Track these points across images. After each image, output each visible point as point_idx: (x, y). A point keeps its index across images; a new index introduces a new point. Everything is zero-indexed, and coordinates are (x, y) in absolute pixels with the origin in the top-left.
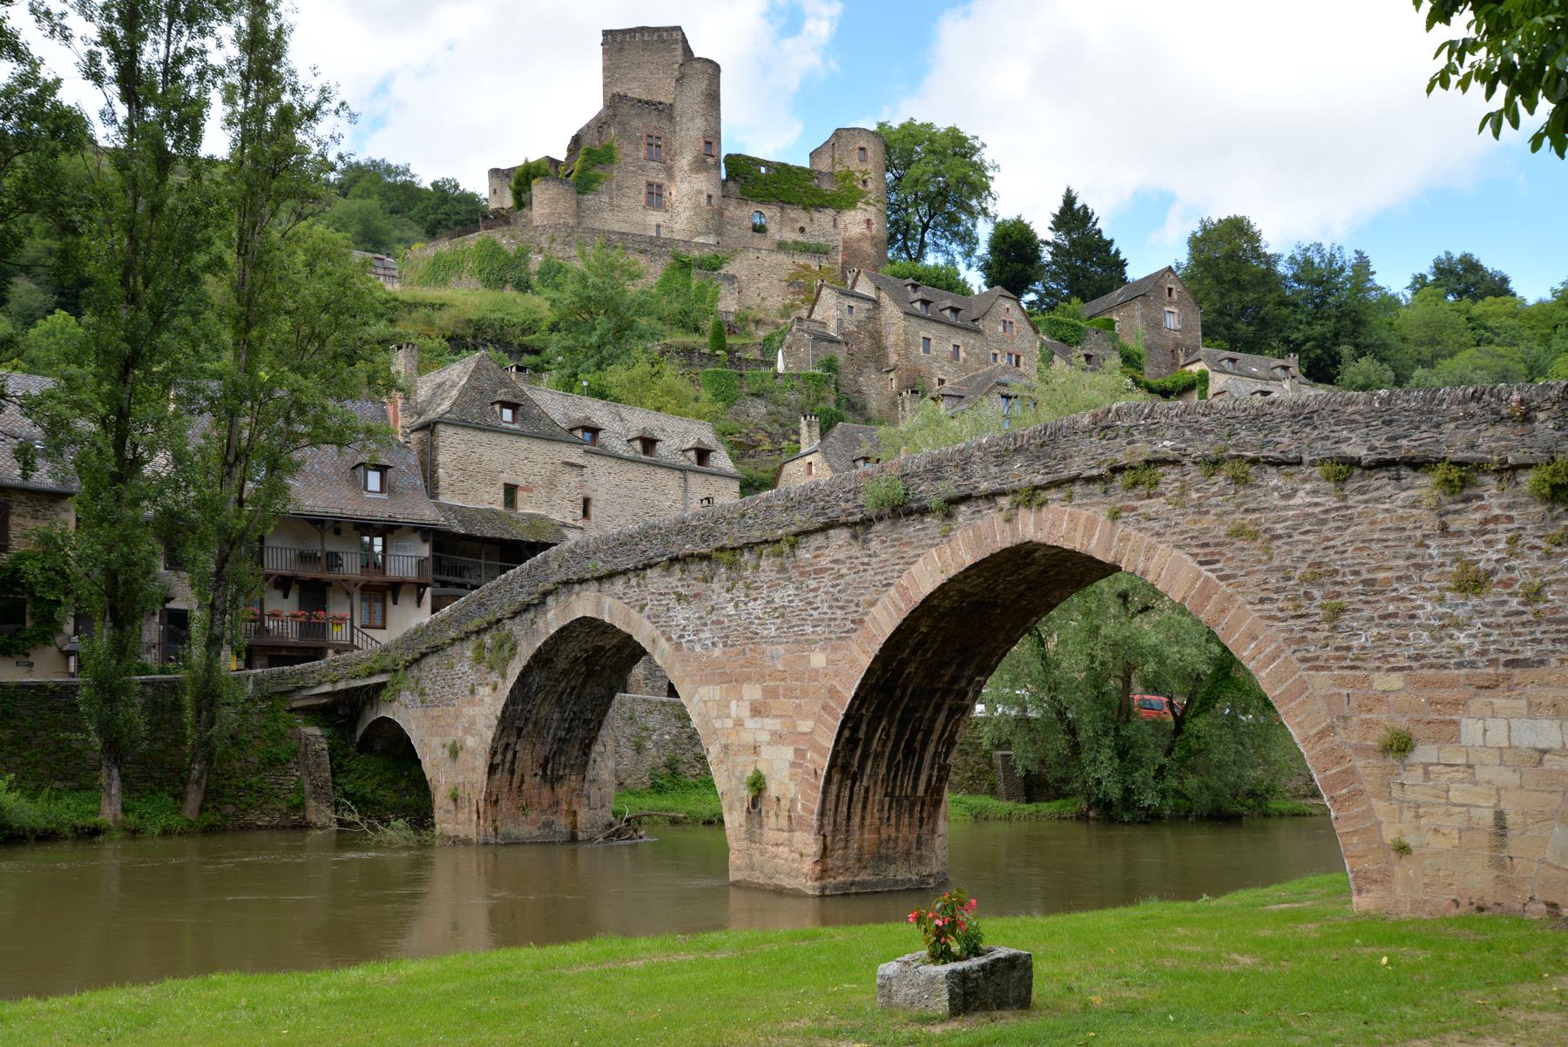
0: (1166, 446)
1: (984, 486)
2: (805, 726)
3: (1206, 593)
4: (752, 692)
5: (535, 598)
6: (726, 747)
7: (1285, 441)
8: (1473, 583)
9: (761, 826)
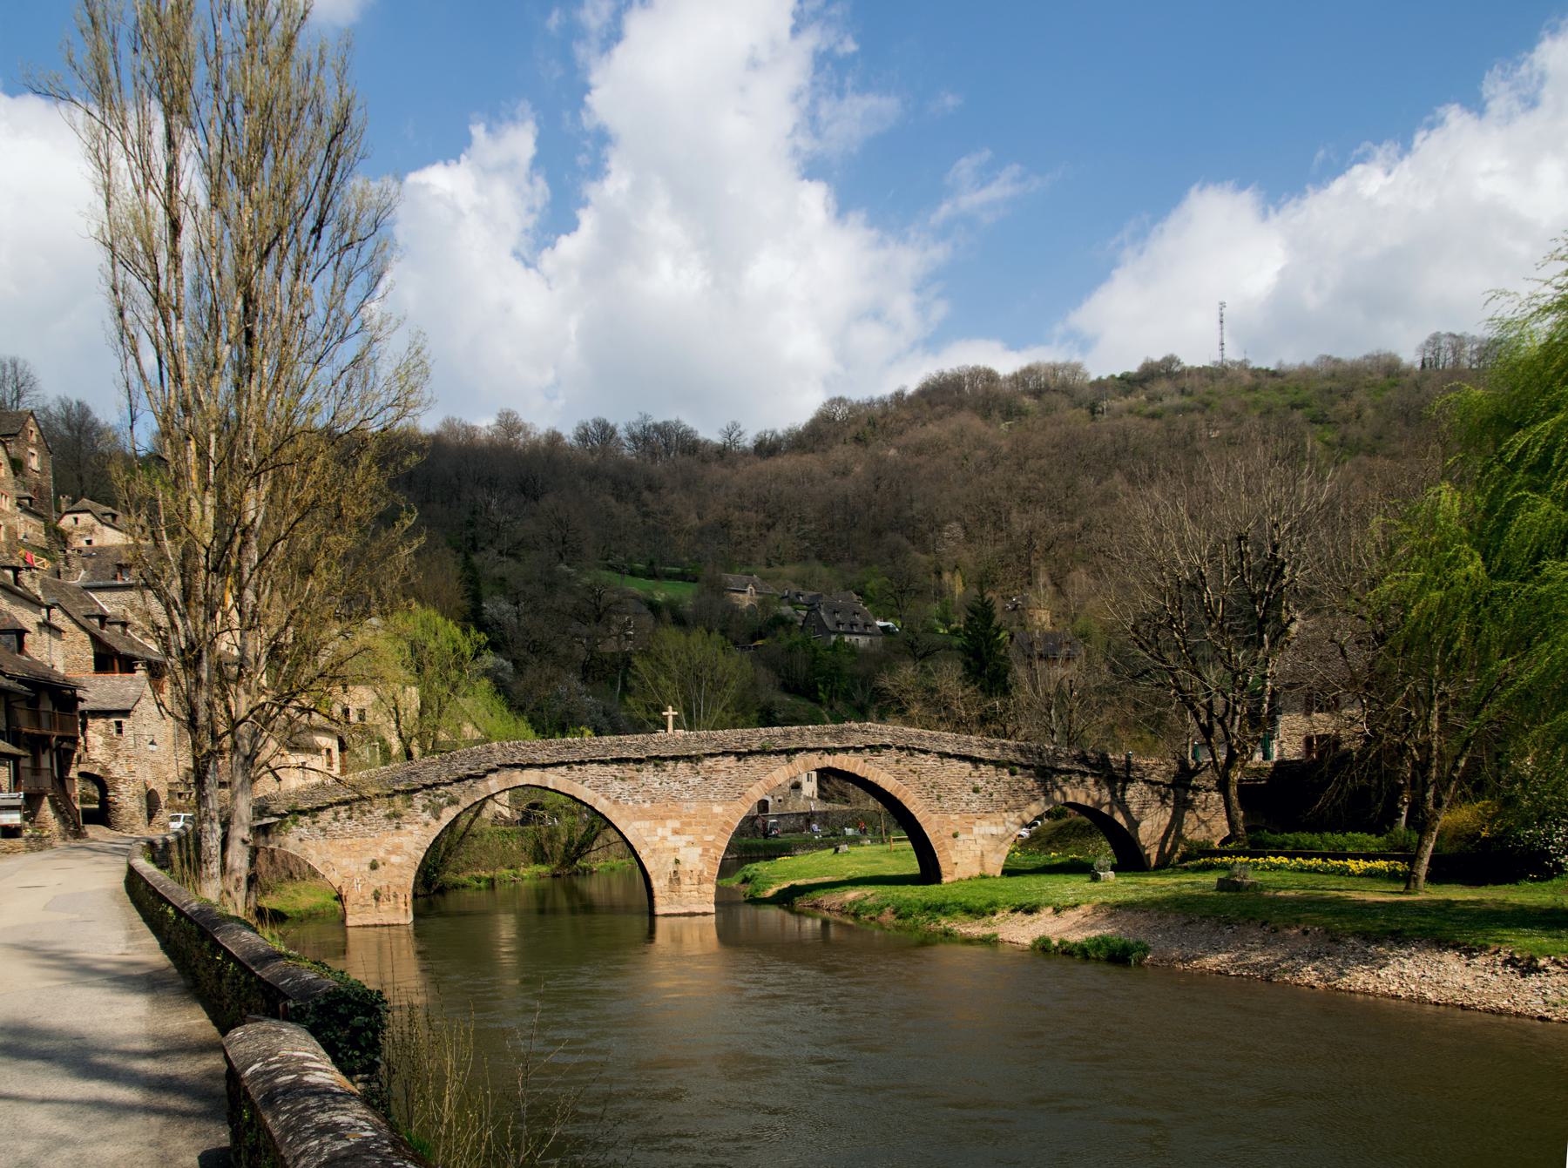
0: (887, 740)
1: (811, 745)
2: (710, 838)
3: (899, 789)
4: (676, 824)
5: (481, 772)
6: (654, 851)
7: (927, 745)
8: (976, 790)
9: (679, 884)
